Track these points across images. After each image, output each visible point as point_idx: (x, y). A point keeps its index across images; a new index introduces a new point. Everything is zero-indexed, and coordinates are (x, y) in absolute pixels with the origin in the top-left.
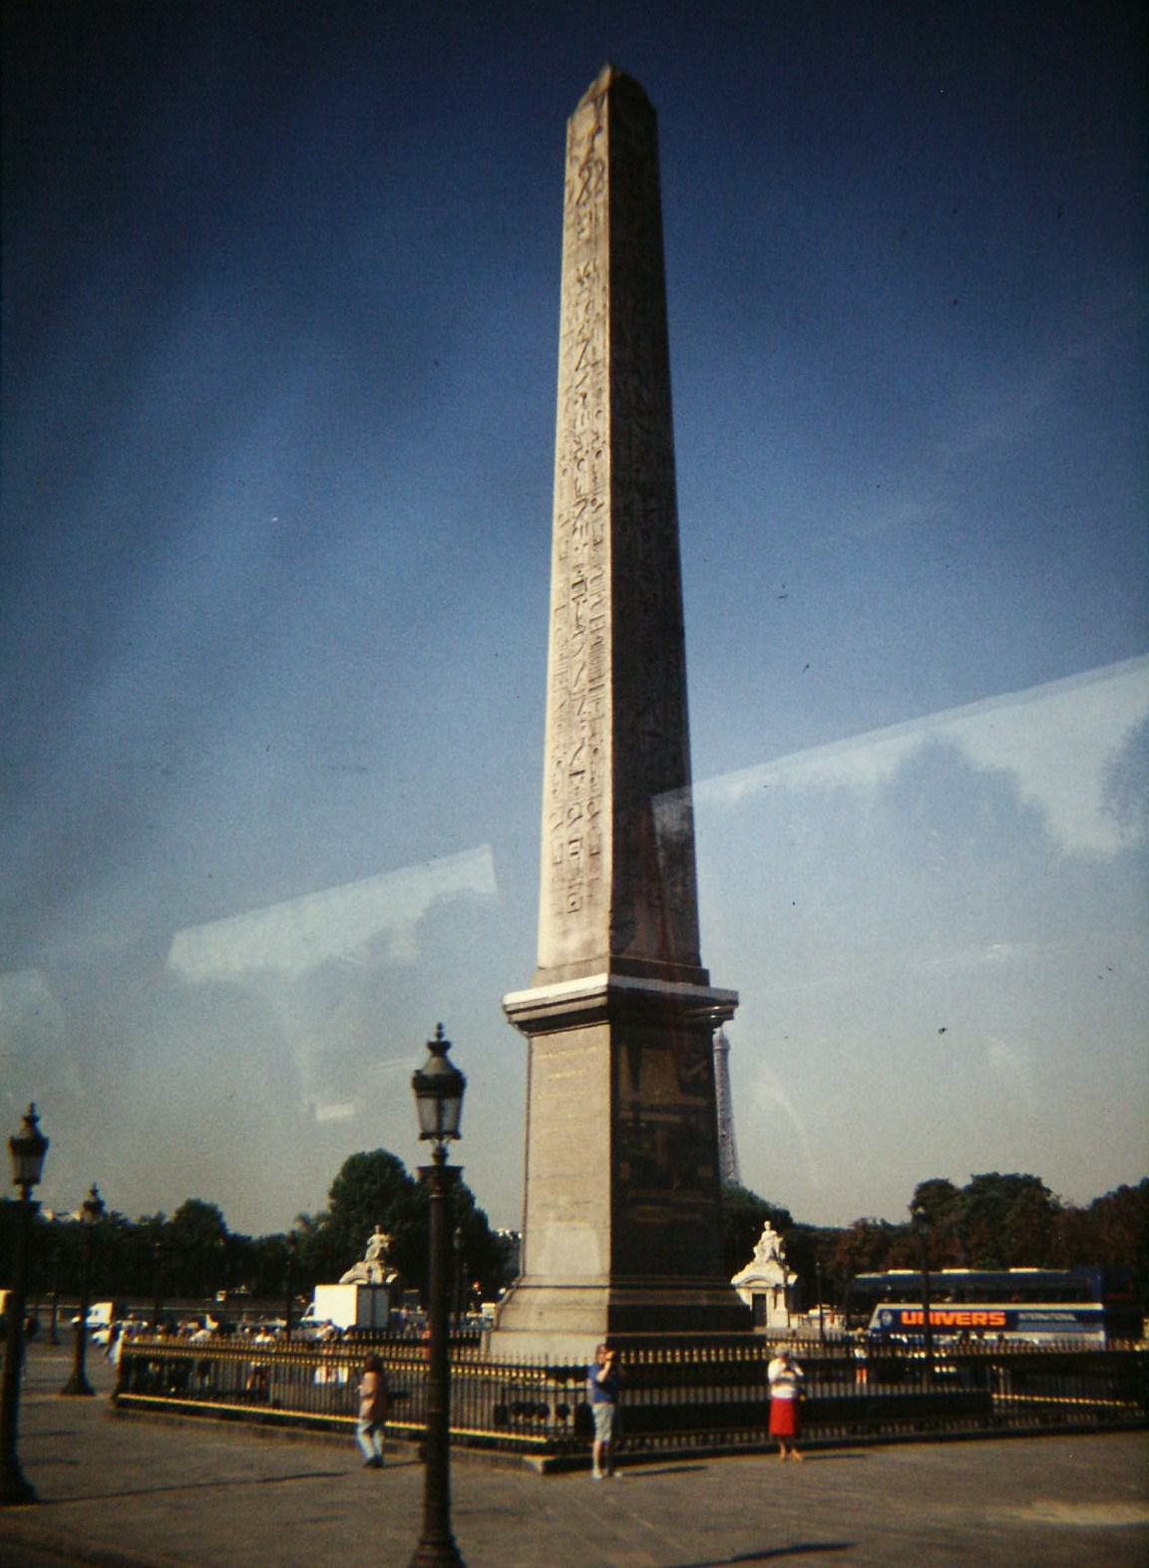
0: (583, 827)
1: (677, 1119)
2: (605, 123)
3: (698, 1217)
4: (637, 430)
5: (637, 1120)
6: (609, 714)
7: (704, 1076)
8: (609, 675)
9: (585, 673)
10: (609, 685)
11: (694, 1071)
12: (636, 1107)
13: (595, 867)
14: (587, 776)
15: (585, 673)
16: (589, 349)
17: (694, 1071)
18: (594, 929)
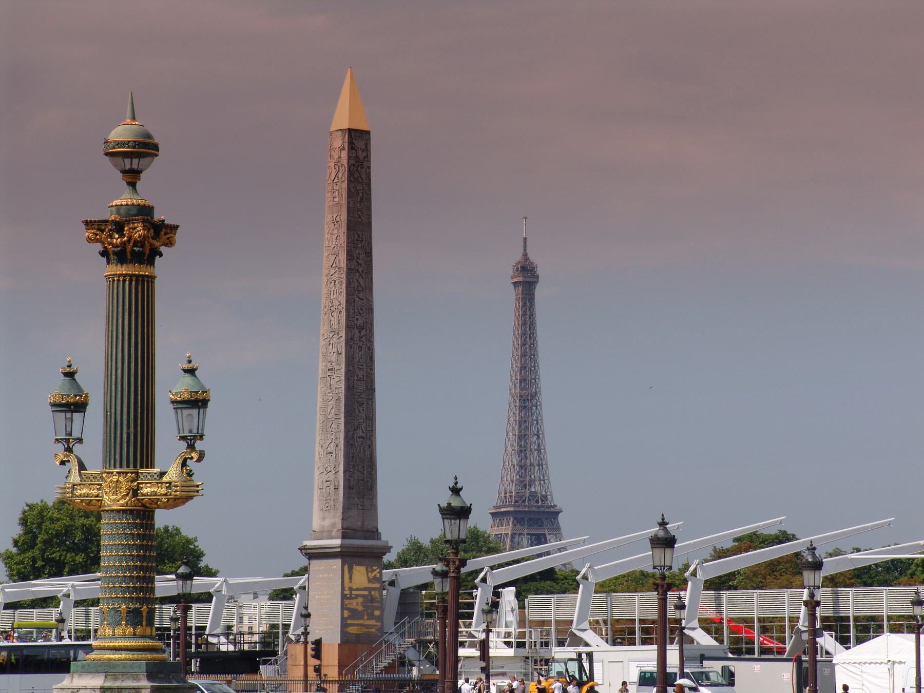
0: (331, 476)
1: (366, 593)
2: (346, 145)
3: (373, 630)
4: (357, 300)
5: (351, 594)
6: (343, 431)
7: (378, 575)
8: (343, 415)
9: (333, 411)
10: (343, 419)
11: (373, 574)
12: (351, 589)
13: (336, 493)
14: (334, 455)
15: (333, 411)
16: (337, 260)
17: (373, 574)
18: (335, 520)
